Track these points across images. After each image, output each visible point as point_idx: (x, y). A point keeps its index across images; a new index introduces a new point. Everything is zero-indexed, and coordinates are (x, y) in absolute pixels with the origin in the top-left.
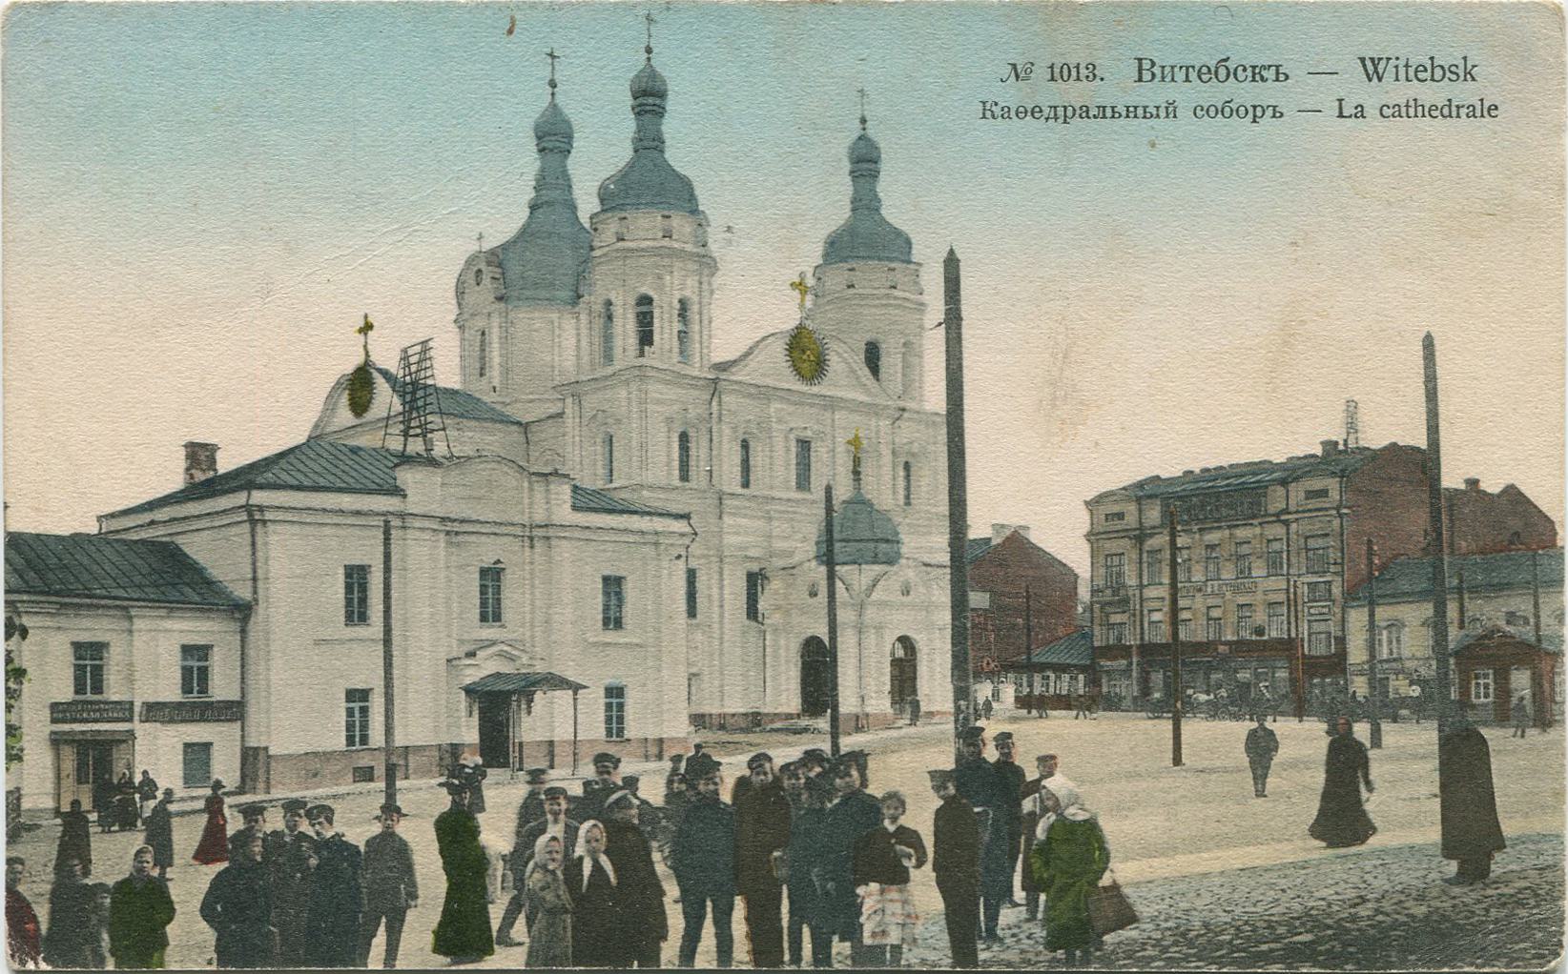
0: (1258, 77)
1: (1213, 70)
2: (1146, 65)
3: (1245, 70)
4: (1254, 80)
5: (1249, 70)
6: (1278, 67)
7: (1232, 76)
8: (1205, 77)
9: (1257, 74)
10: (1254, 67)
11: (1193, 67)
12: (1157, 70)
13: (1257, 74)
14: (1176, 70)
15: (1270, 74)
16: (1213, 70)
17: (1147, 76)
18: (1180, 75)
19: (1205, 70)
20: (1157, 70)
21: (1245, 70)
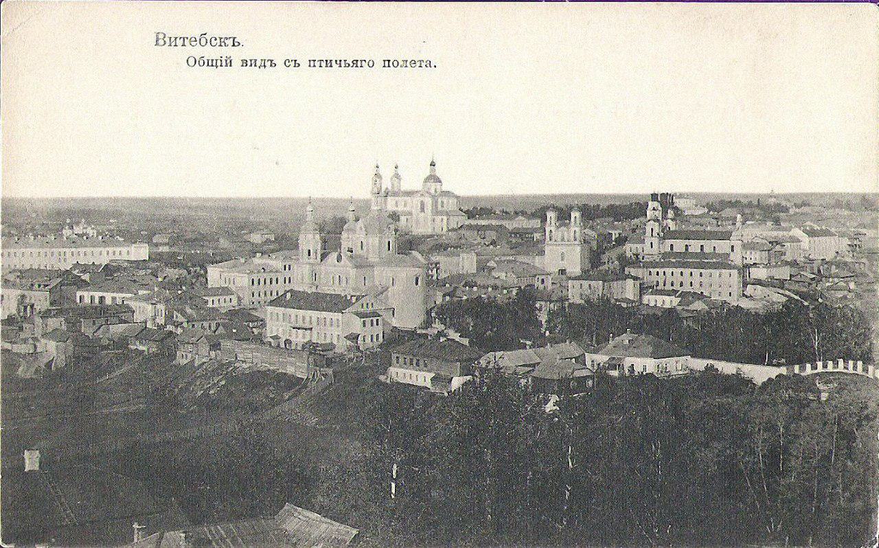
0: (223, 44)
1: (198, 40)
2: (161, 36)
3: (216, 39)
4: (221, 45)
5: (218, 39)
6: (234, 38)
7: (209, 41)
8: (193, 43)
9: (222, 42)
10: (221, 39)
11: (187, 38)
12: (167, 40)
13: (222, 42)
14: (178, 39)
15: (230, 42)
16: (198, 40)
17: (161, 42)
18: (180, 42)
19: (193, 39)
20: (167, 40)
21: (216, 39)
